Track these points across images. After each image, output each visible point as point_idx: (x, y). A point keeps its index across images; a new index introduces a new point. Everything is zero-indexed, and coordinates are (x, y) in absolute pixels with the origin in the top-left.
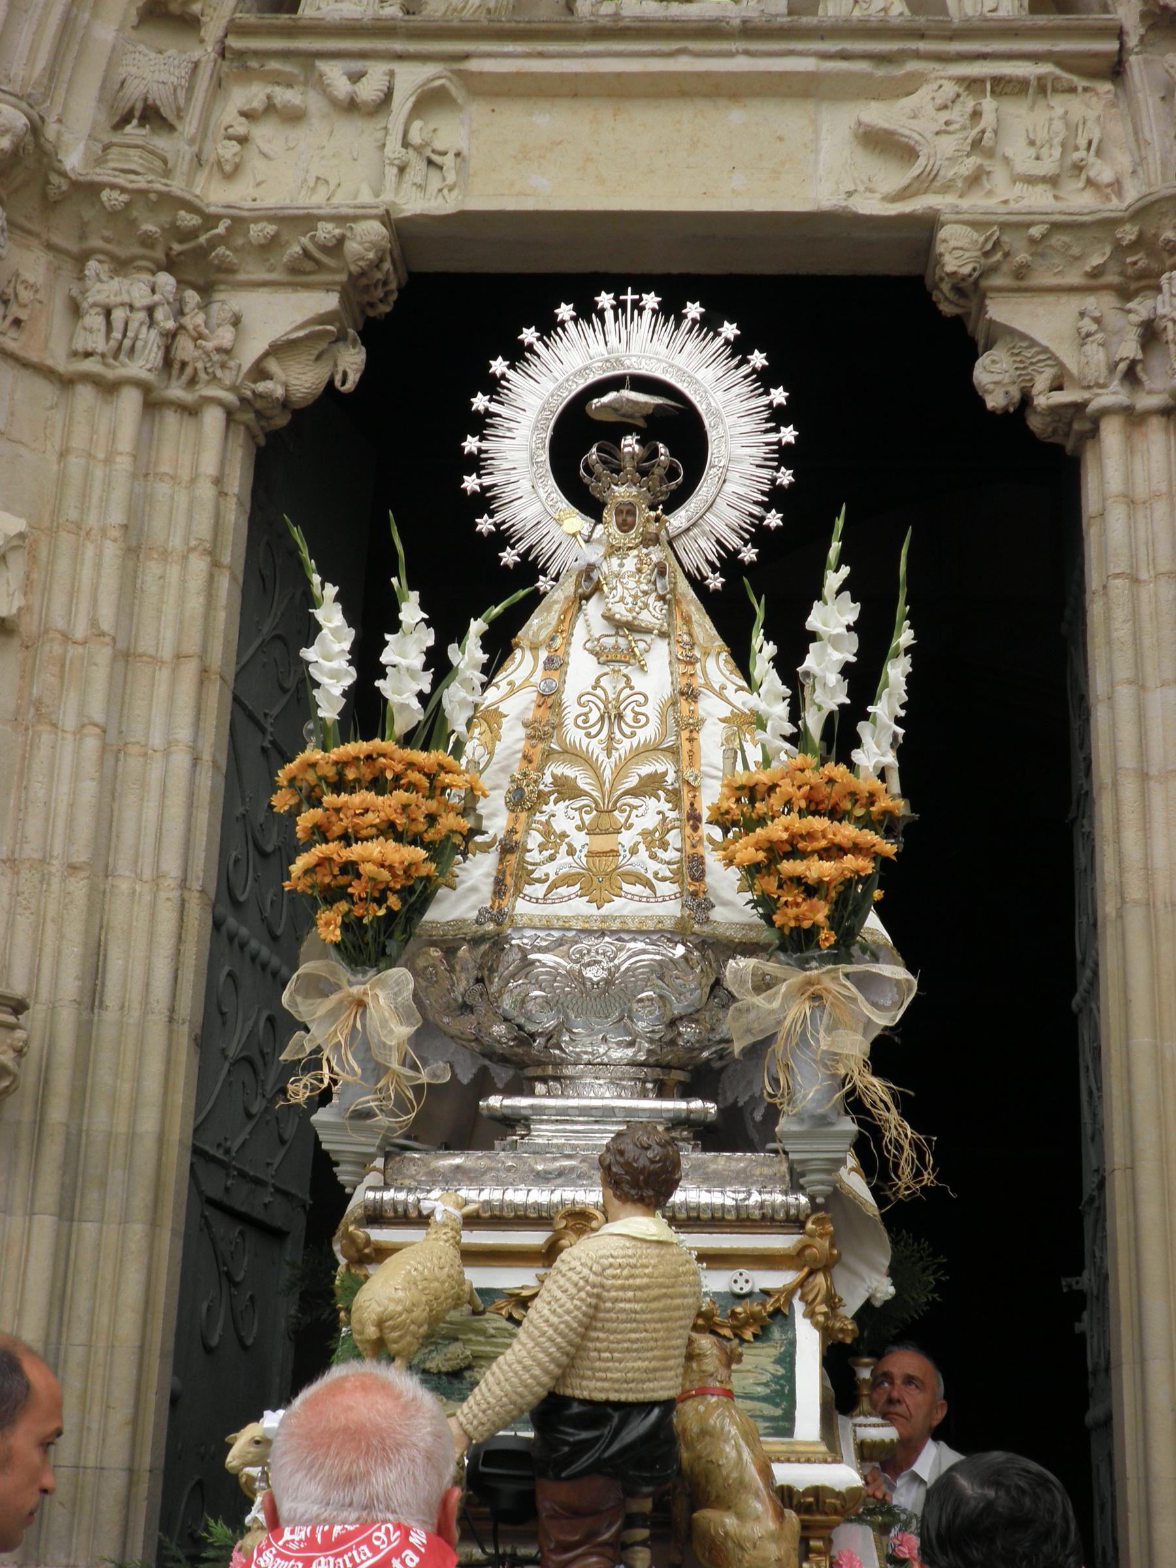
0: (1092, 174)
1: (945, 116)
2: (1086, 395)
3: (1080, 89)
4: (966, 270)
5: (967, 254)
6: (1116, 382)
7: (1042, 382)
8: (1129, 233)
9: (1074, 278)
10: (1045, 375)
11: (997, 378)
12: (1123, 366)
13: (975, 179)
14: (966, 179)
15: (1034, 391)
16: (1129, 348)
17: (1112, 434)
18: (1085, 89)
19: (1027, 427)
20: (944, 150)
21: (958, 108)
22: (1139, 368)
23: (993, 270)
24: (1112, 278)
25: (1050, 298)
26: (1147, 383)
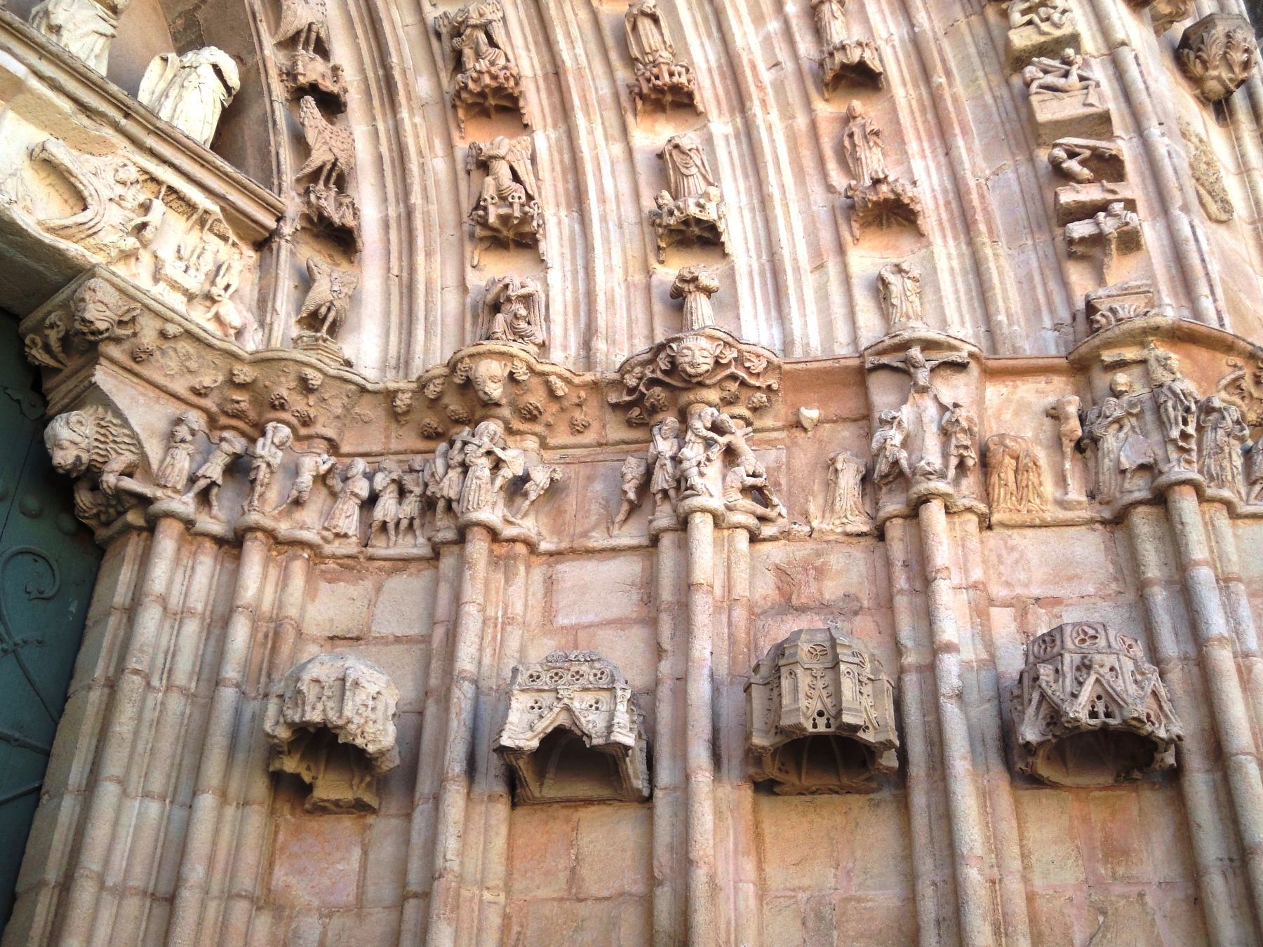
0: (222, 312)
1: (119, 190)
2: (159, 493)
3: (230, 241)
4: (101, 326)
5: (108, 313)
6: (191, 494)
8: (245, 373)
9: (180, 387)
10: (122, 458)
11: (78, 439)
12: (202, 483)
13: (126, 256)
14: (122, 251)
15: (107, 468)
16: (214, 470)
17: (167, 541)
18: (234, 244)
19: (73, 498)
20: (110, 220)
21: (134, 190)
22: (215, 490)
23: (118, 340)
24: (209, 403)
25: (152, 393)
26: (215, 510)
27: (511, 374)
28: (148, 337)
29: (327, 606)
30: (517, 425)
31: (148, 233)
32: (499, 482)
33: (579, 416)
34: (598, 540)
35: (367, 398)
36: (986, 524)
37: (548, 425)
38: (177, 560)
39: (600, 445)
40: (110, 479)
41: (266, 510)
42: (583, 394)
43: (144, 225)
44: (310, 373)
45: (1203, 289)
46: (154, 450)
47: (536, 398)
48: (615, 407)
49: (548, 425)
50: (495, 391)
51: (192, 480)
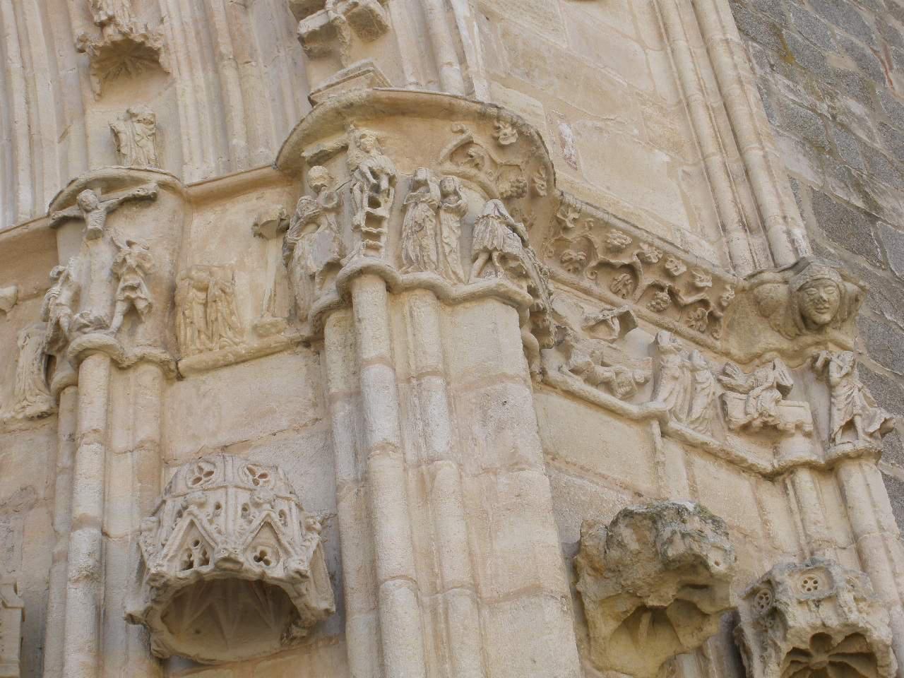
36: (173, 374)
45: (447, 55)
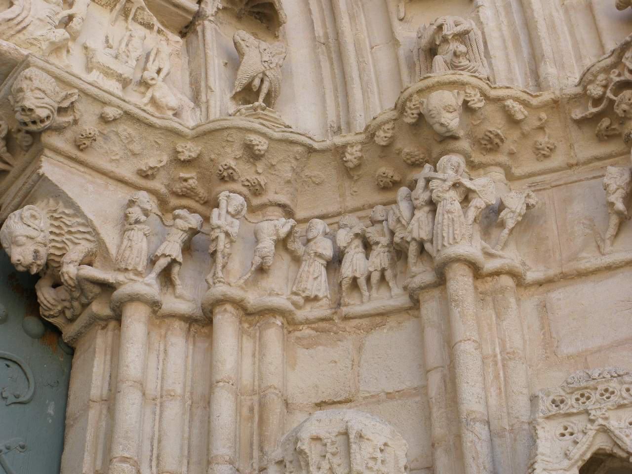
0: (157, 95)
2: (121, 277)
3: (156, 28)
4: (43, 113)
5: (47, 100)
6: (153, 275)
7: (75, 253)
8: (189, 150)
9: (127, 171)
10: (79, 247)
11: (33, 233)
12: (163, 263)
13: (57, 48)
14: (52, 43)
15: (66, 259)
16: (173, 248)
17: (136, 322)
18: (159, 31)
19: (36, 297)
22: (176, 269)
23: (59, 129)
24: (157, 185)
25: (100, 180)
26: (179, 289)
27: (466, 102)
28: (89, 124)
29: (308, 371)
30: (477, 158)
31: (75, 24)
32: (472, 213)
33: (543, 139)
34: (590, 260)
35: (315, 159)
37: (511, 154)
38: (149, 345)
39: (570, 166)
40: (70, 270)
41: (232, 279)
42: (543, 115)
43: (71, 18)
44: (255, 139)
46: (110, 237)
47: (495, 124)
48: (581, 123)
49: (511, 154)
50: (452, 121)
51: (152, 262)
